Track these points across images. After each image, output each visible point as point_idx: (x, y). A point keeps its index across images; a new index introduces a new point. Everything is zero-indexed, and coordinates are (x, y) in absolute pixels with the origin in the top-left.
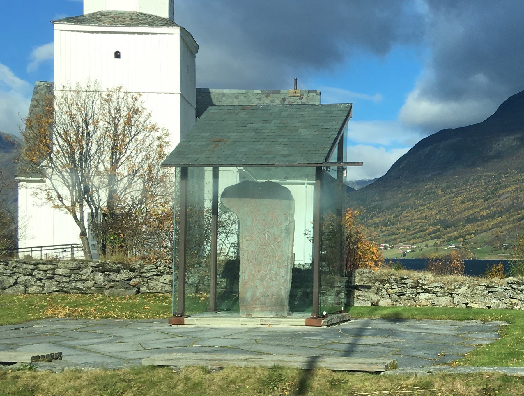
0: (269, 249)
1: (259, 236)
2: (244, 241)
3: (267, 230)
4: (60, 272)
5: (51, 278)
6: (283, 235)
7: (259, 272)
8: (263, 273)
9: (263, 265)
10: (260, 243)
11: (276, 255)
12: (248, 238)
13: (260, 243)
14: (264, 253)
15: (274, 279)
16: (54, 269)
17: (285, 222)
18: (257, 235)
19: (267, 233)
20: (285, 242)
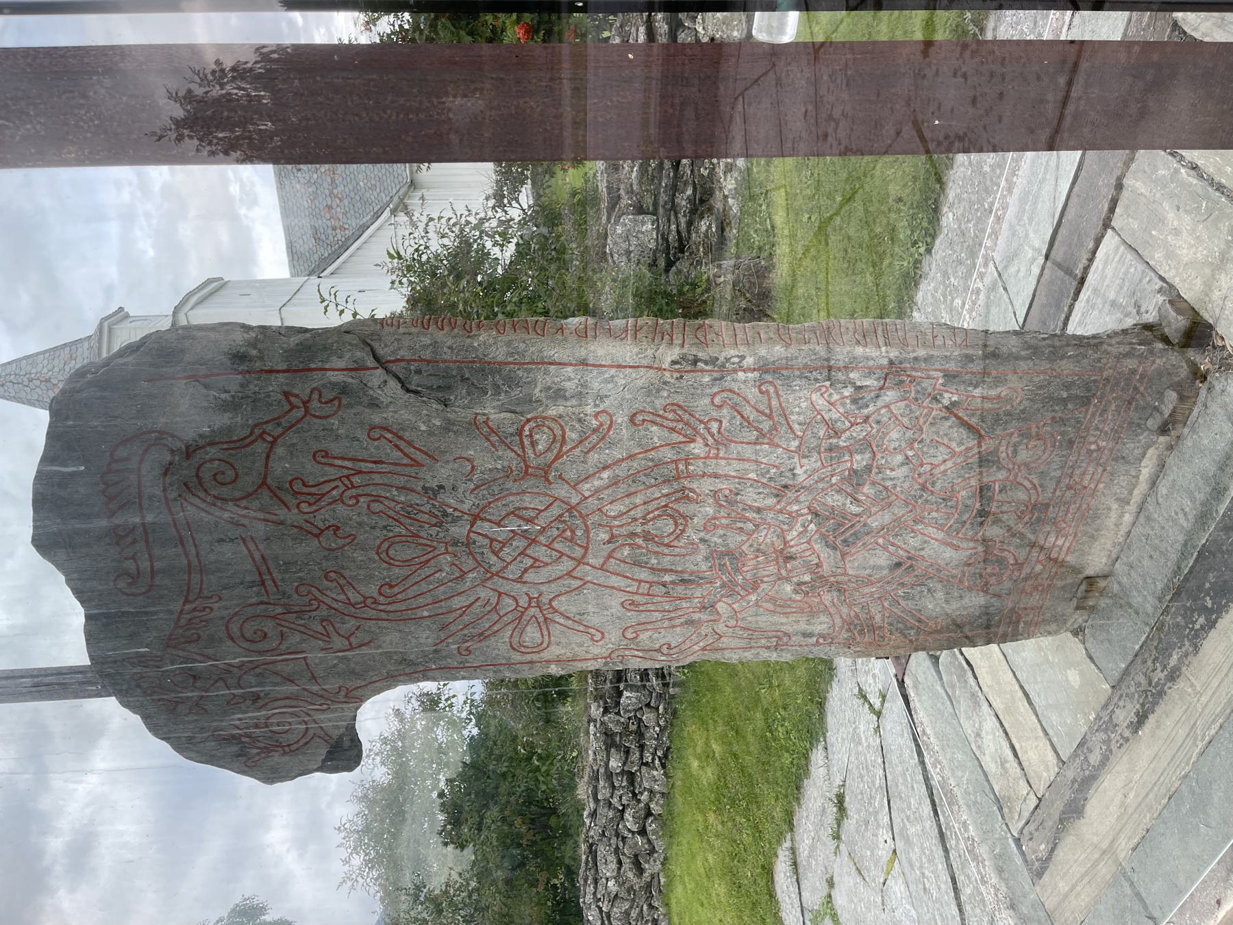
0: (613, 510)
1: (513, 571)
2: (555, 651)
3: (459, 531)
4: (615, 764)
5: (631, 777)
6: (491, 410)
7: (791, 558)
8: (802, 537)
9: (734, 540)
10: (567, 565)
11: (669, 454)
12: (532, 634)
13: (567, 565)
14: (647, 537)
15: (860, 461)
16: (609, 776)
17: (374, 404)
18: (505, 587)
19: (484, 527)
20: (558, 394)
